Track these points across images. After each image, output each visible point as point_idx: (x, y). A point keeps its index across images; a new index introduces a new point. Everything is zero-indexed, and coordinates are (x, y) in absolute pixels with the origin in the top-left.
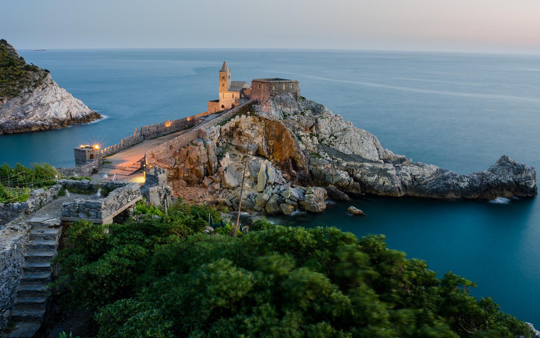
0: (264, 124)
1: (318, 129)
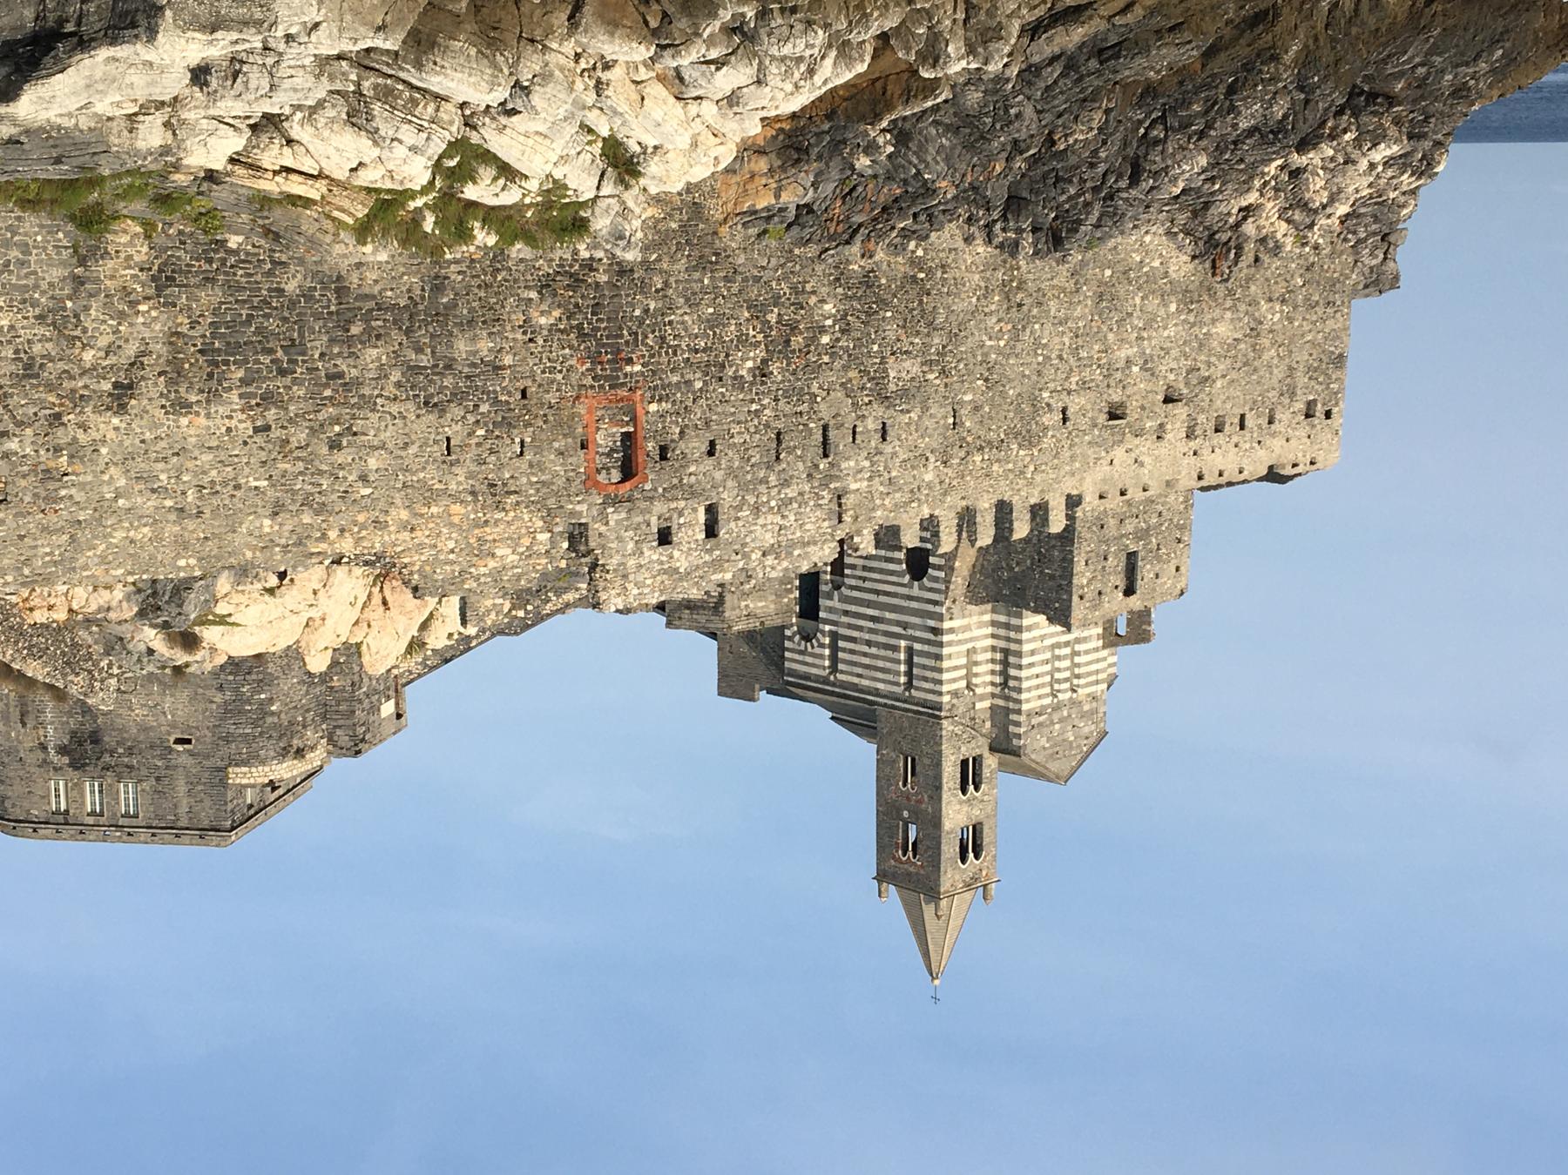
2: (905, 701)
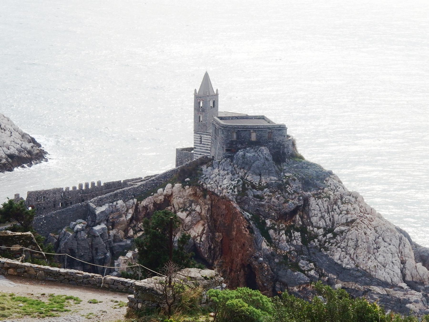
0: (209, 202)
1: (309, 218)
2: (201, 134)
